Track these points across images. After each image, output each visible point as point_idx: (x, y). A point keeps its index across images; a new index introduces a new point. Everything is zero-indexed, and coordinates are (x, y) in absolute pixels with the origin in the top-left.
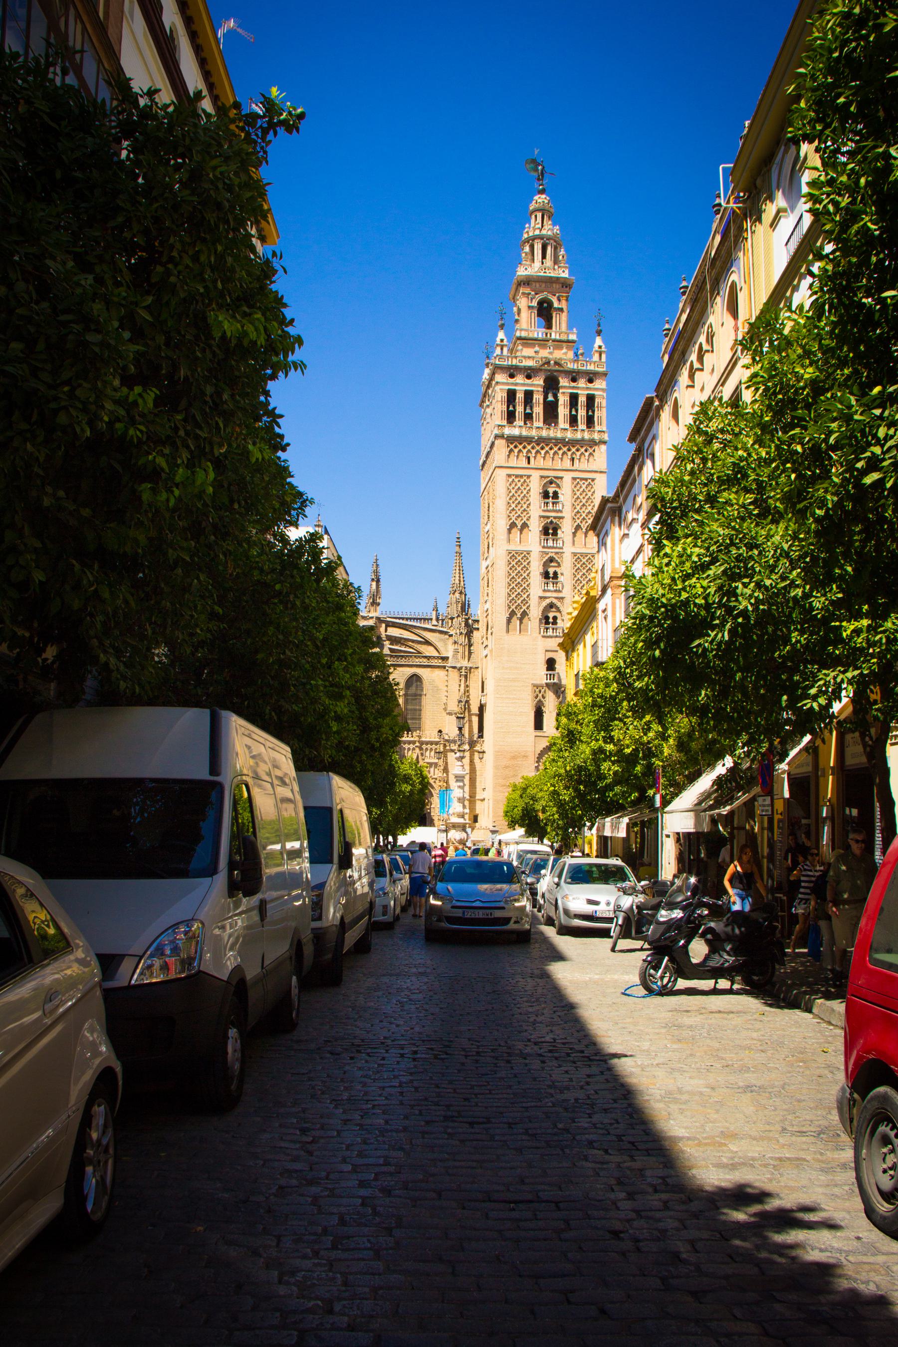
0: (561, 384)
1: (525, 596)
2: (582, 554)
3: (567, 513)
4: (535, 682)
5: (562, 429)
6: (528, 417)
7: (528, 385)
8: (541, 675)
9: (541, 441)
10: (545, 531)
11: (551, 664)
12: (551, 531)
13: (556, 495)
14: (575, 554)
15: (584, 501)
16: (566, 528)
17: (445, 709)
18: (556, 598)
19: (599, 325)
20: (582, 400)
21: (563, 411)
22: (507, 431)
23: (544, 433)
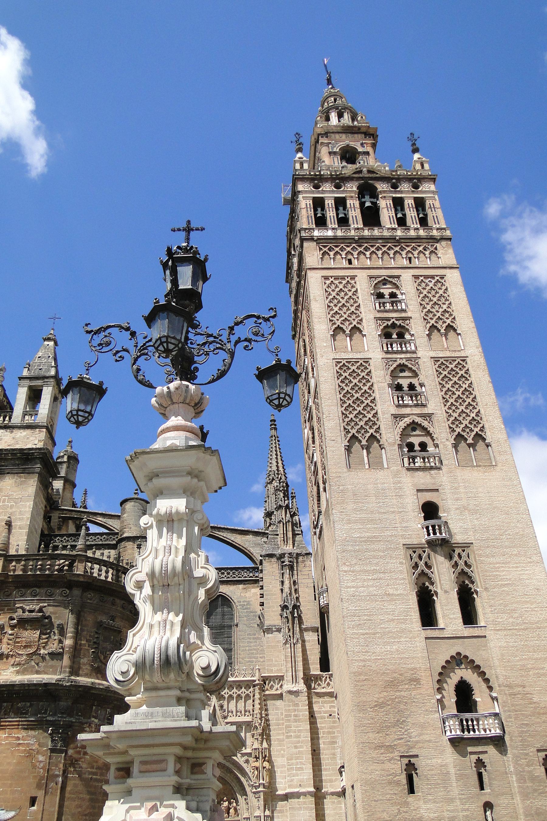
0: (379, 190)
1: (370, 416)
2: (447, 359)
6: (343, 222)
8: (416, 530)
12: (395, 336)
13: (393, 295)
14: (436, 360)
15: (435, 299)
16: (417, 328)
17: (261, 625)
19: (414, 144)
20: (409, 202)
21: (387, 215)
22: (316, 233)
23: (366, 233)
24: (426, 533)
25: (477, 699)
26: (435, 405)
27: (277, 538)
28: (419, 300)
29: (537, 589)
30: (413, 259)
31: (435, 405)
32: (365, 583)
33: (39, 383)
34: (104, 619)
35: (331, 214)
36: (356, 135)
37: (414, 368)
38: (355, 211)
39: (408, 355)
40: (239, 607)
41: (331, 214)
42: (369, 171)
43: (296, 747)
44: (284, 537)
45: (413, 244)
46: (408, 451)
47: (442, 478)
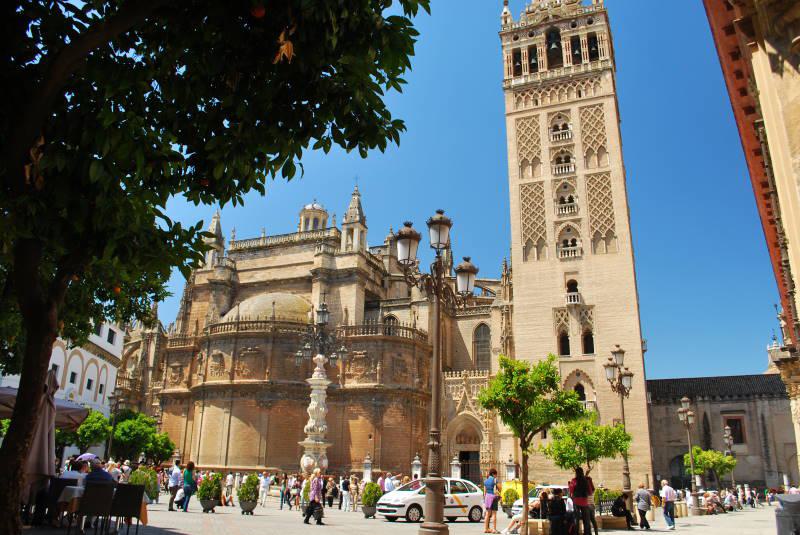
0: (562, 32)
3: (577, 140)
4: (555, 306)
5: (568, 68)
6: (533, 68)
7: (531, 41)
8: (562, 298)
9: (547, 85)
10: (558, 160)
12: (563, 160)
14: (588, 176)
15: (593, 126)
16: (578, 154)
18: (573, 221)
21: (566, 53)
22: (513, 83)
23: (549, 76)
26: (583, 213)
33: (351, 226)
34: (395, 355)
42: (554, 16)
47: (581, 265)
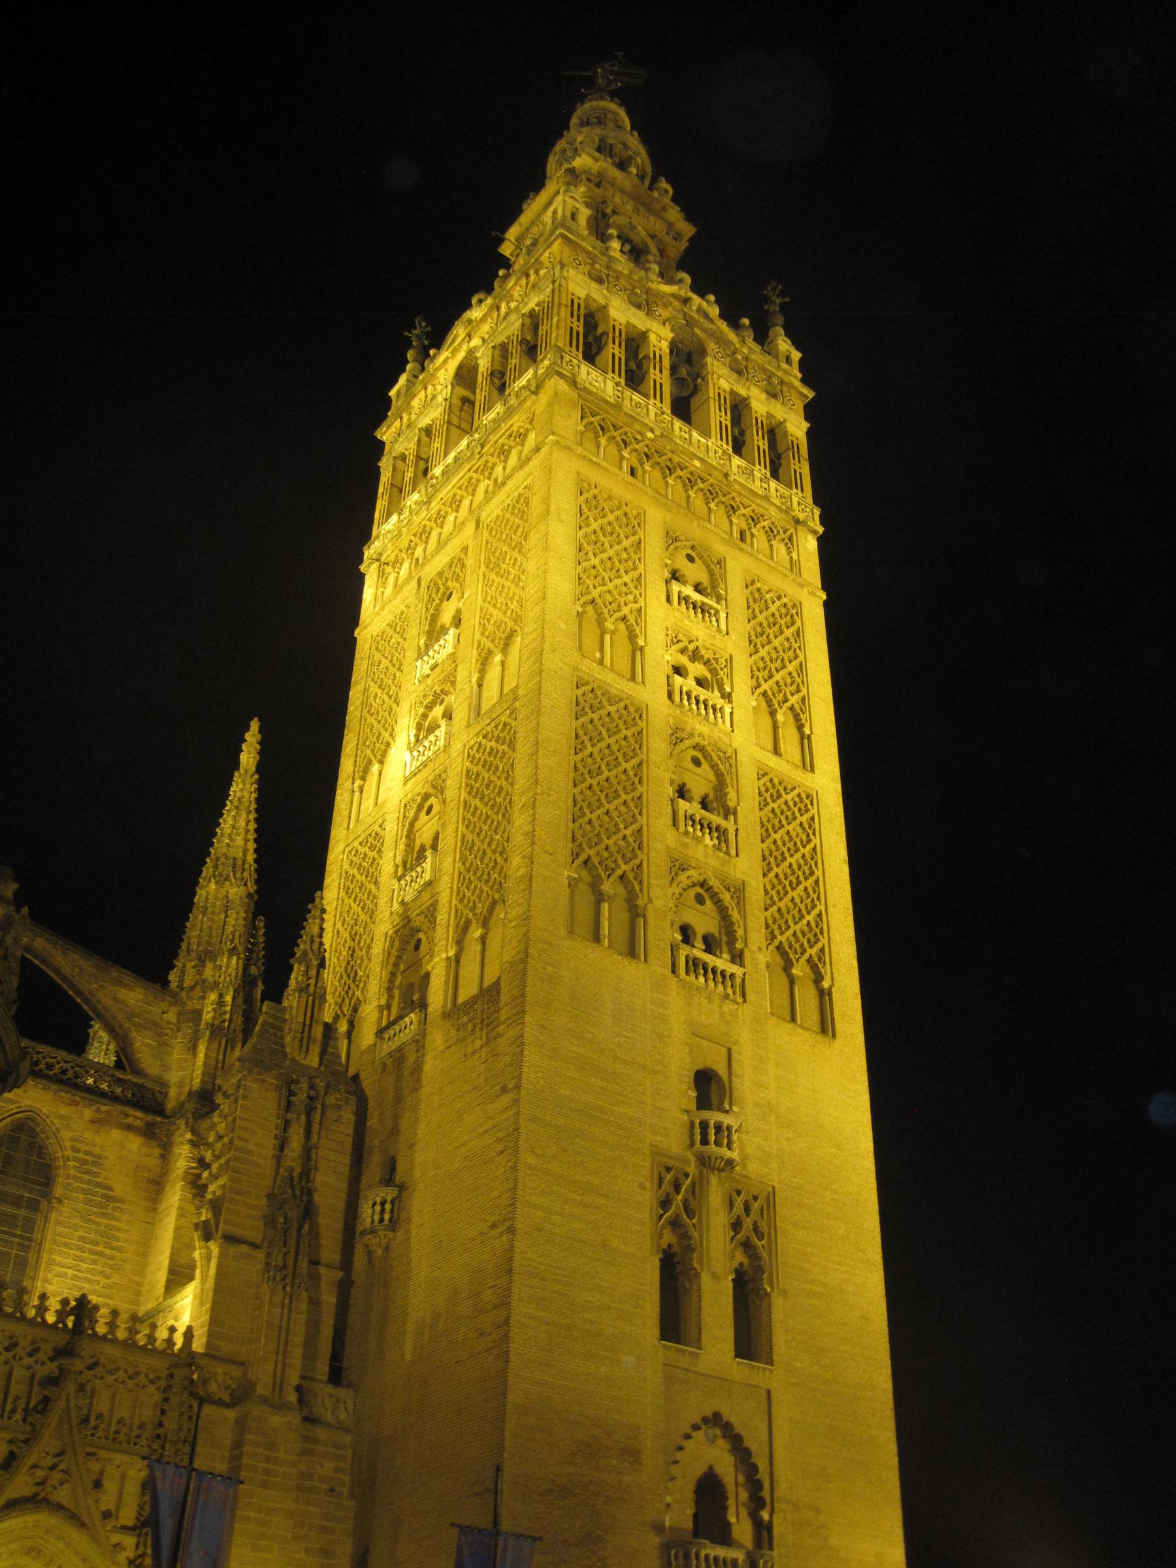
11: (709, 1087)
24: (698, 1138)
25: (732, 1519)
27: (282, 1030)
28: (749, 627)
29: (867, 1319)
30: (748, 534)
31: (746, 866)
32: (566, 1207)
35: (616, 351)
36: (652, 219)
37: (721, 767)
38: (661, 372)
39: (717, 734)
40: (72, 1164)
41: (616, 351)
43: (256, 1548)
44: (302, 1033)
45: (754, 506)
46: (682, 941)
